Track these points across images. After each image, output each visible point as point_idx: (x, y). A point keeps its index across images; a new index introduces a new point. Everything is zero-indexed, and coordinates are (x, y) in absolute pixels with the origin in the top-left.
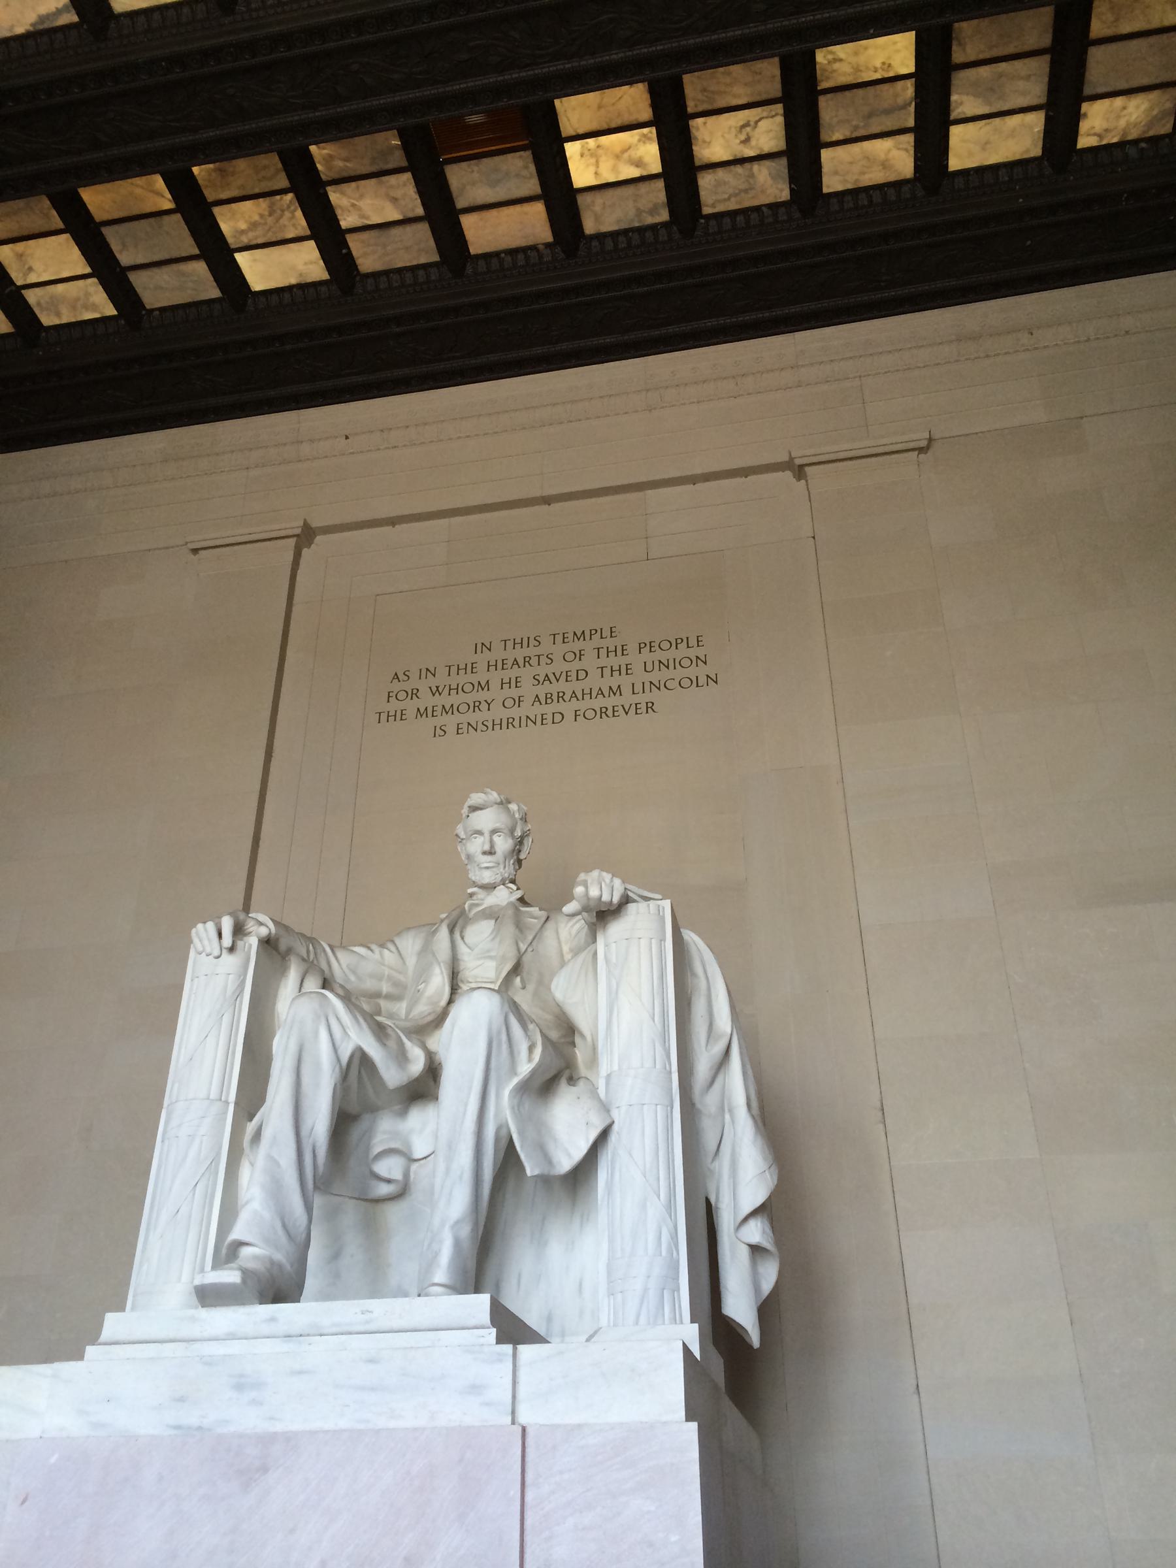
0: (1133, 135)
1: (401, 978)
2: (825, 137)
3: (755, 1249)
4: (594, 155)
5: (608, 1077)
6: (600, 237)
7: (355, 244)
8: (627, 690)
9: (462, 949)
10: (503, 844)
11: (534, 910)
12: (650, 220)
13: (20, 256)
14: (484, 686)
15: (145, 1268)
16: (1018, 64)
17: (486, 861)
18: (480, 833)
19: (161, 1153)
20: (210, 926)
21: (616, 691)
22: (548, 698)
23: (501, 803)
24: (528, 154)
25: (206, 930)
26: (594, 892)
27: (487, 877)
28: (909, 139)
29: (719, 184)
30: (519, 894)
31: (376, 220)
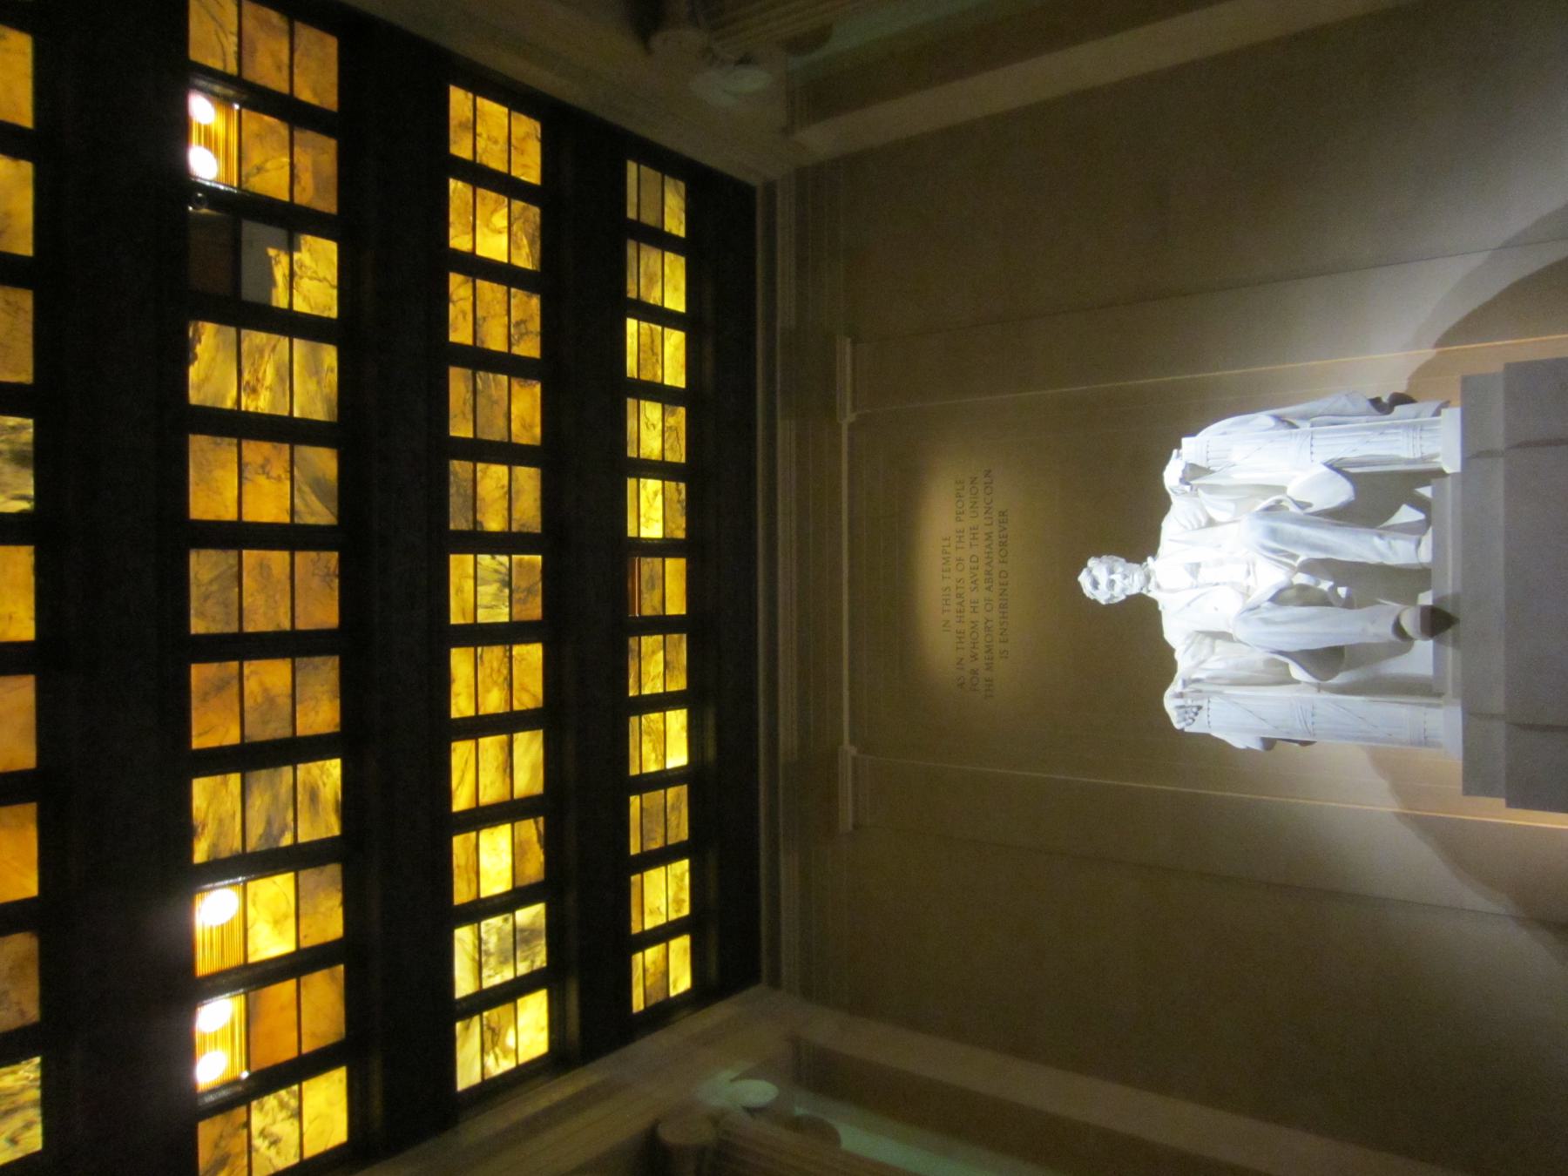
0: (682, 205)
2: (659, 380)
4: (648, 520)
6: (688, 529)
7: (672, 688)
8: (988, 530)
12: (683, 496)
13: (651, 912)
14: (974, 623)
16: (642, 263)
21: (989, 536)
22: (987, 581)
24: (643, 560)
28: (667, 331)
29: (672, 448)
30: (1150, 559)
31: (661, 668)
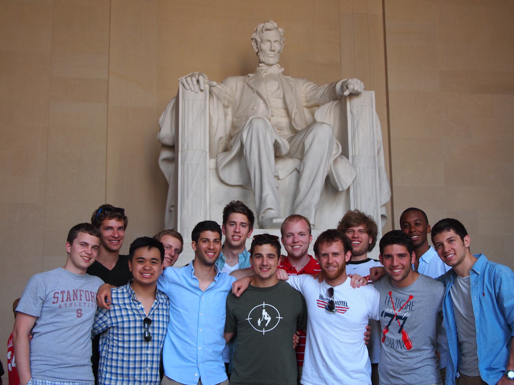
1: (231, 99)
3: (383, 216)
5: (353, 157)
9: (269, 94)
10: (277, 47)
11: (290, 77)
15: (185, 211)
17: (271, 54)
18: (270, 41)
19: (183, 170)
20: (194, 79)
23: (277, 28)
25: (192, 80)
26: (356, 88)
27: (272, 61)
30: (283, 70)
